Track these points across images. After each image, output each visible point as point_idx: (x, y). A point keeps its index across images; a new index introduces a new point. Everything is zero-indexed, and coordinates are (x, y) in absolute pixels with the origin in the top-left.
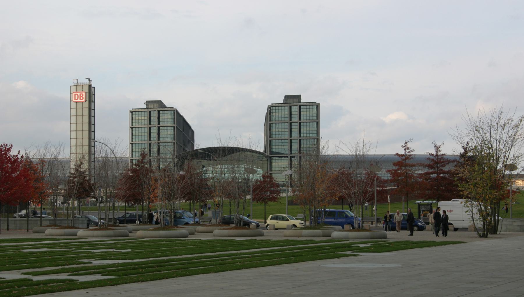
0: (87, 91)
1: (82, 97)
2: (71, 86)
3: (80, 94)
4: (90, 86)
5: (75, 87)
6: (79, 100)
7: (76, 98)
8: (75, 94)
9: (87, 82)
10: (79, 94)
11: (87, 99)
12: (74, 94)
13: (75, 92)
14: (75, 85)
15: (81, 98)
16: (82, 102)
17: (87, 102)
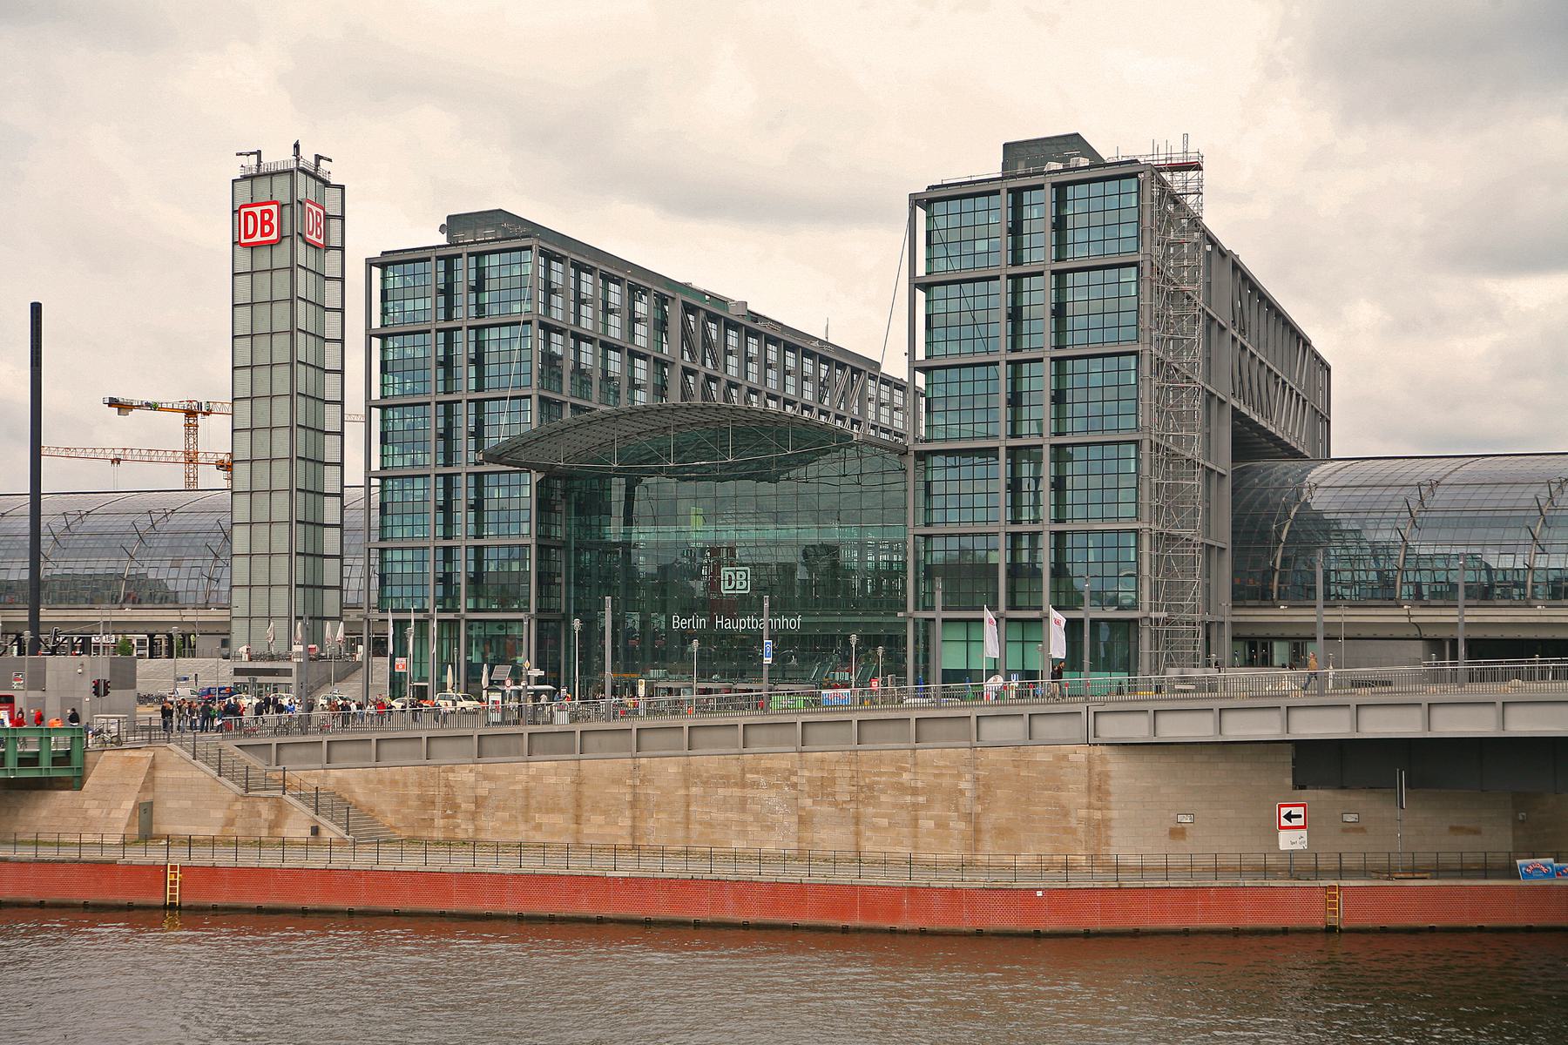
3: (263, 212)
5: (248, 183)
6: (258, 238)
7: (250, 232)
8: (246, 214)
10: (257, 210)
11: (287, 232)
15: (267, 229)
16: (271, 244)
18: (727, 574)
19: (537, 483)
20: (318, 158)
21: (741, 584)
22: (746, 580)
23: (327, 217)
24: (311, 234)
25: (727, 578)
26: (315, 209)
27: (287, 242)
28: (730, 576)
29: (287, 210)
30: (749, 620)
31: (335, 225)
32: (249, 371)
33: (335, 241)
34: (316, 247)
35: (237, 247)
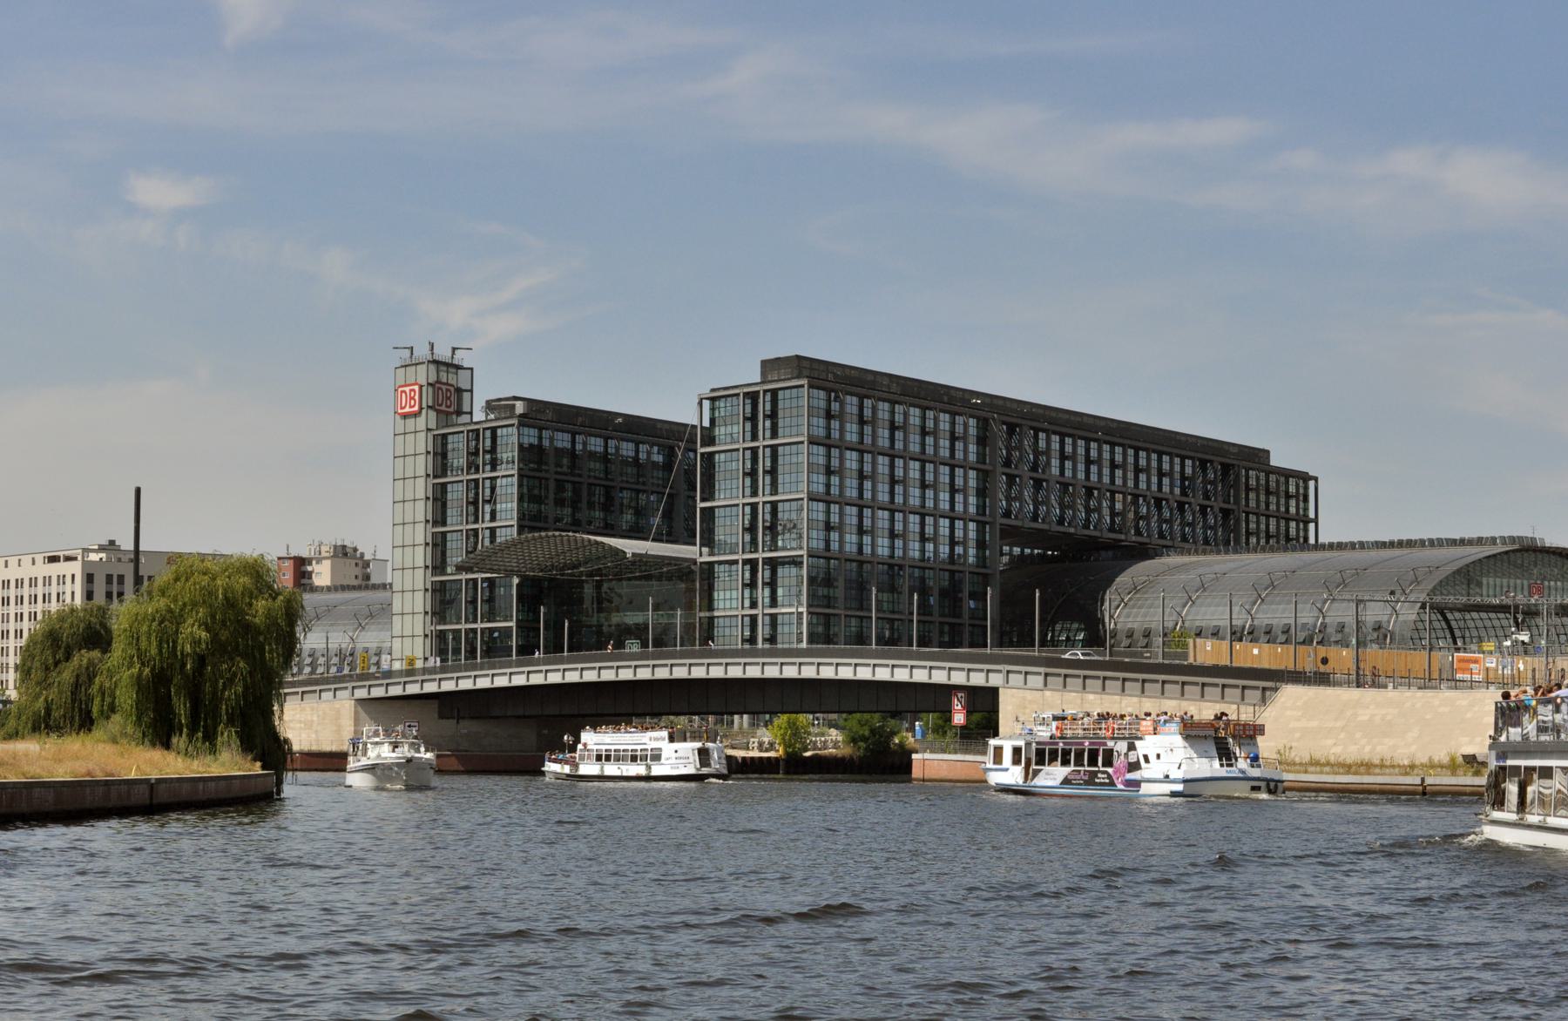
3: (411, 390)
6: (407, 410)
10: (407, 389)
11: (424, 405)
12: (400, 389)
13: (403, 383)
15: (413, 402)
16: (416, 415)
19: (517, 585)
20: (454, 349)
23: (459, 391)
24: (441, 405)
26: (444, 387)
27: (424, 412)
29: (424, 389)
31: (466, 396)
33: (466, 408)
34: (448, 414)
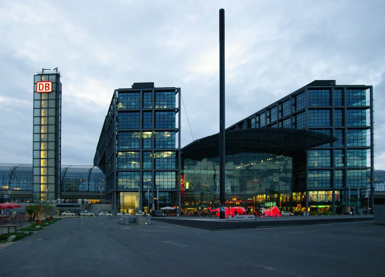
0: (54, 81)
1: (48, 87)
2: (35, 75)
3: (46, 84)
4: (58, 76)
5: (39, 77)
6: (44, 90)
7: (41, 89)
8: (40, 84)
9: (55, 72)
10: (44, 83)
11: (54, 89)
13: (40, 81)
14: (40, 74)
15: (47, 88)
16: (48, 93)
17: (54, 93)
18: (231, 181)
21: (235, 183)
22: (237, 182)
25: (231, 181)
28: (232, 181)
30: (238, 192)
32: (39, 124)
35: (35, 93)
